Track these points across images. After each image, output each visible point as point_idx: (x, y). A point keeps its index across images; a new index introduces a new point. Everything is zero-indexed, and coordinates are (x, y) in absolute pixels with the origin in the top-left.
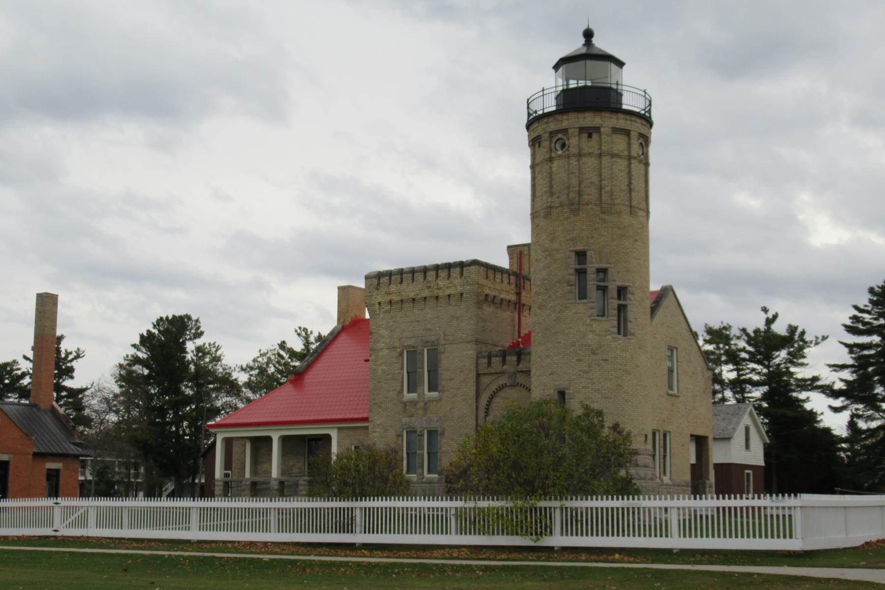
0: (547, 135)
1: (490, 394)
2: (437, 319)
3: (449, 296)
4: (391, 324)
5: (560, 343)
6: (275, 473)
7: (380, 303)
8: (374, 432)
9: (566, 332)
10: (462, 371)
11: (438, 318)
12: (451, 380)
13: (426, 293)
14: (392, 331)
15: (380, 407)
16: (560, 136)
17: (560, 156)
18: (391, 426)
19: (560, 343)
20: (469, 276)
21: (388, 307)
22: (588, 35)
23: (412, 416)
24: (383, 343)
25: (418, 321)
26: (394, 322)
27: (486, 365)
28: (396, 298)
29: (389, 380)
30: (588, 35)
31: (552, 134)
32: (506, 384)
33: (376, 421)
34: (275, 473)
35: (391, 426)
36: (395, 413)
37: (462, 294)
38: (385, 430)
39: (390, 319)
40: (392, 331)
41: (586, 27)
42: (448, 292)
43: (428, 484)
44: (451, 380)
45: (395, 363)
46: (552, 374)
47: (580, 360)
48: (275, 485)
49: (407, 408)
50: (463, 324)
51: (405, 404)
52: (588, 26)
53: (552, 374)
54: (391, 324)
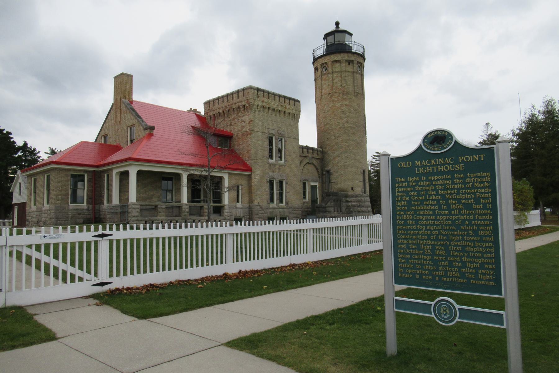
0: (356, 62)
3: (289, 113)
7: (258, 105)
8: (255, 178)
10: (294, 153)
11: (284, 123)
12: (290, 156)
13: (280, 108)
14: (262, 123)
15: (258, 164)
21: (262, 109)
22: (337, 24)
24: (258, 128)
25: (275, 121)
26: (263, 118)
28: (267, 106)
29: (262, 150)
30: (337, 24)
35: (263, 176)
36: (266, 169)
37: (294, 114)
38: (261, 178)
39: (262, 116)
40: (262, 123)
41: (336, 21)
42: (290, 111)
43: (282, 209)
44: (290, 156)
46: (361, 163)
48: (186, 208)
49: (271, 167)
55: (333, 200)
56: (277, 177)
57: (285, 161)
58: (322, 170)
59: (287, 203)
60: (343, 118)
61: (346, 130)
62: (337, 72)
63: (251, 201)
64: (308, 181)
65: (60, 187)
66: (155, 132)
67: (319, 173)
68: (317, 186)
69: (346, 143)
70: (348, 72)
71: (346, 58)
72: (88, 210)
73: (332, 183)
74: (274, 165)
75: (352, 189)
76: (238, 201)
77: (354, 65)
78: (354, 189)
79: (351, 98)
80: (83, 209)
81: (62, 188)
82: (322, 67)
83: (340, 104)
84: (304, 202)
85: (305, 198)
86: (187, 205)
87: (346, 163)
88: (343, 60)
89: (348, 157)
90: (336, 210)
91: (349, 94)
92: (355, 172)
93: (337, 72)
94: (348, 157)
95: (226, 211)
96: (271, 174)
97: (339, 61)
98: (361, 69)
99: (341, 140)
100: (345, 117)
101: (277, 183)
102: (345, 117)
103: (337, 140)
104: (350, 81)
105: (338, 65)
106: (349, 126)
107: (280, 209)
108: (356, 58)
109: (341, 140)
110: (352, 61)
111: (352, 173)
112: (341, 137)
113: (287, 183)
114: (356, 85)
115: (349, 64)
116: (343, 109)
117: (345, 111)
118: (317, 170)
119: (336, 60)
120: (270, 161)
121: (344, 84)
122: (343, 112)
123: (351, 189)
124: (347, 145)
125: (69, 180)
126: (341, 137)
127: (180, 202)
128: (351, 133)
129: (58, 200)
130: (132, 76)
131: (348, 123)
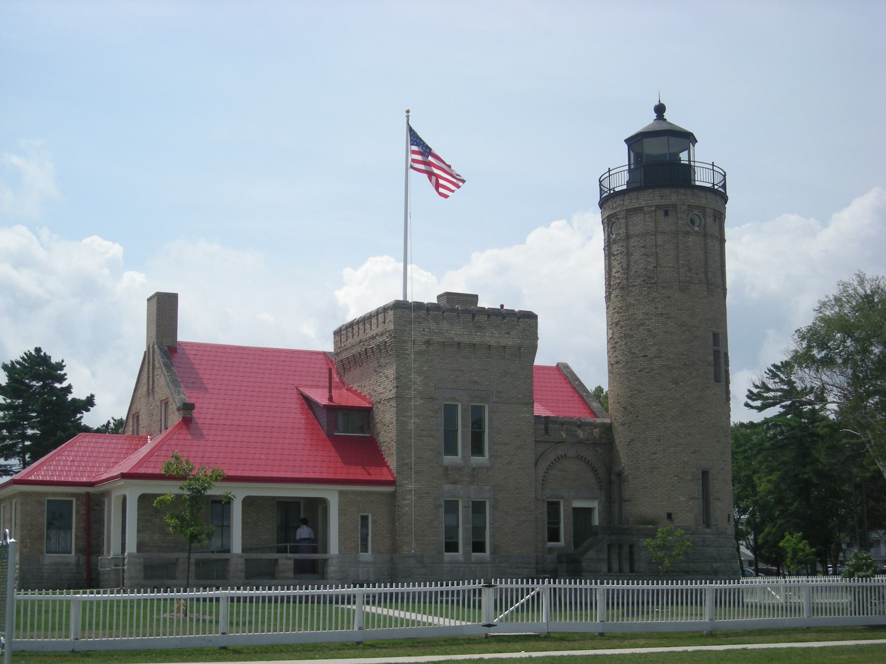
0: (685, 207)
1: (548, 464)
2: (486, 372)
3: (504, 347)
4: (425, 369)
5: (703, 421)
6: (237, 546)
9: (708, 411)
12: (506, 444)
13: (477, 340)
16: (696, 212)
17: (696, 232)
18: (428, 493)
19: (703, 421)
20: (529, 330)
21: (423, 347)
22: (660, 109)
23: (455, 483)
25: (462, 371)
27: (543, 432)
28: (436, 339)
30: (660, 109)
31: (691, 207)
32: (565, 455)
33: (407, 486)
34: (237, 546)
37: (520, 348)
41: (657, 103)
42: (503, 342)
45: (432, 417)
46: (694, 452)
47: (719, 442)
50: (518, 383)
51: (446, 469)
52: (660, 101)
53: (694, 452)
54: (425, 369)
55: (606, 545)
56: (464, 494)
57: (491, 456)
58: (610, 471)
59: (494, 552)
60: (650, 345)
61: (656, 374)
62: (637, 236)
63: (394, 548)
64: (563, 498)
65: (29, 524)
66: (195, 413)
67: (599, 478)
68: (595, 508)
69: (655, 405)
70: (664, 233)
71: (657, 201)
72: (77, 564)
73: (626, 503)
74: (458, 469)
75: (669, 516)
76: (365, 549)
77: (679, 215)
78: (673, 516)
79: (669, 297)
80: (68, 564)
81: (31, 525)
82: (611, 224)
83: (643, 313)
84: (551, 550)
85: (554, 535)
86: (241, 557)
87: (655, 453)
88: (651, 207)
89: (660, 440)
90: (615, 567)
91: (663, 287)
92: (677, 476)
93: (637, 236)
94: (659, 440)
95: (332, 569)
96: (447, 487)
97: (638, 210)
98: (703, 220)
99: (645, 399)
100: (654, 344)
101: (464, 507)
102: (654, 344)
103: (637, 398)
104: (669, 255)
105: (638, 218)
106: (664, 365)
107: (471, 565)
108: (683, 198)
109: (645, 399)
110: (675, 206)
111: (670, 479)
112: (644, 391)
113: (494, 507)
114: (683, 264)
115: (666, 213)
116: (648, 325)
117: (655, 329)
118: (595, 471)
119: (635, 206)
120: (448, 460)
121: (653, 263)
122: (649, 331)
123: (666, 516)
124: (658, 411)
125: (44, 511)
126: (644, 391)
127: (228, 551)
128: (669, 382)
129: (25, 547)
130: (177, 294)
131: (662, 357)
